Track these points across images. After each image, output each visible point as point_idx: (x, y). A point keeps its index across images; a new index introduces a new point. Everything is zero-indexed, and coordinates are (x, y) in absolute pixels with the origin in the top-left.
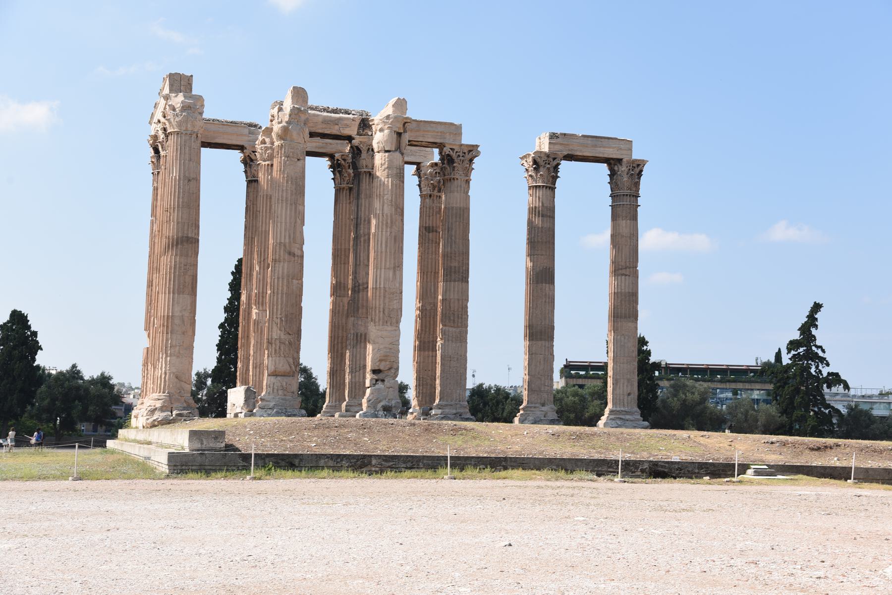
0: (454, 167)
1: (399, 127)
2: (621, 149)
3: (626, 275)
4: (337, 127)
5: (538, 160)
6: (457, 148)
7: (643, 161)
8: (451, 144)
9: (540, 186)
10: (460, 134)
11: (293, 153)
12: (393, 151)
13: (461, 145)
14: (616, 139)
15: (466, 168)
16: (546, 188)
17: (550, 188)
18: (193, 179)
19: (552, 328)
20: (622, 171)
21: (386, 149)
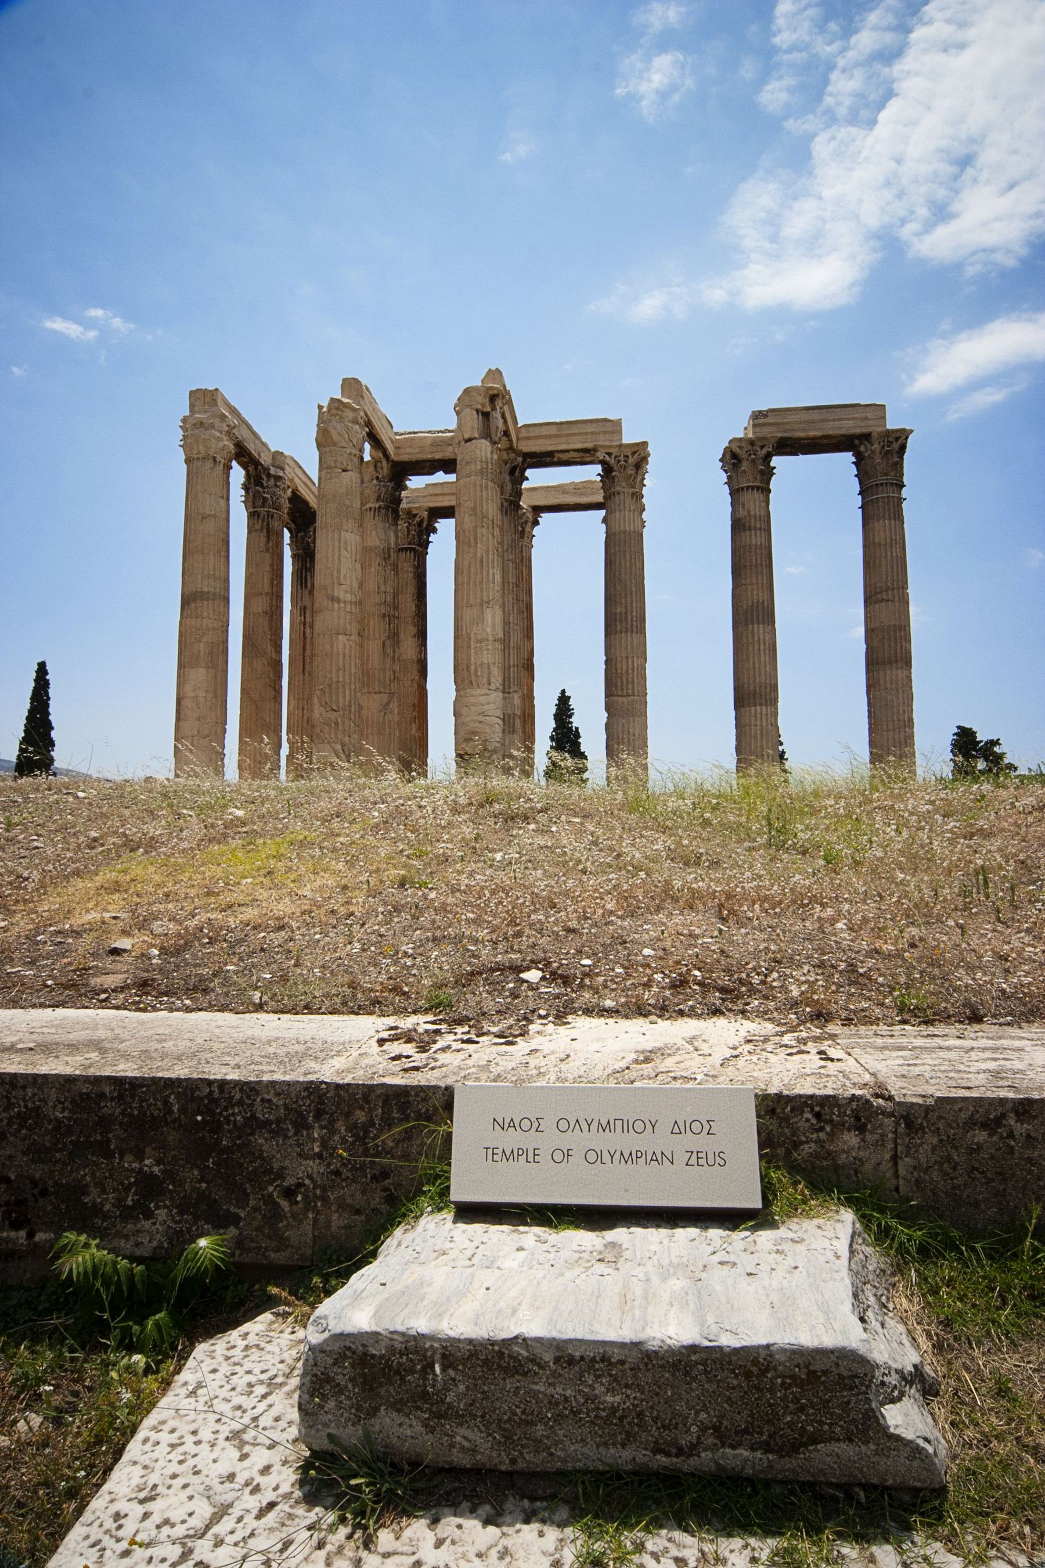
0: (613, 478)
1: (481, 402)
2: (867, 418)
3: (887, 601)
4: (450, 448)
5: (738, 451)
6: (615, 451)
7: (904, 430)
8: (605, 447)
9: (743, 489)
10: (620, 432)
11: (336, 461)
12: (476, 438)
13: (621, 446)
14: (858, 405)
15: (631, 475)
16: (753, 489)
17: (758, 488)
18: (209, 515)
19: (775, 688)
20: (873, 452)
21: (467, 436)
